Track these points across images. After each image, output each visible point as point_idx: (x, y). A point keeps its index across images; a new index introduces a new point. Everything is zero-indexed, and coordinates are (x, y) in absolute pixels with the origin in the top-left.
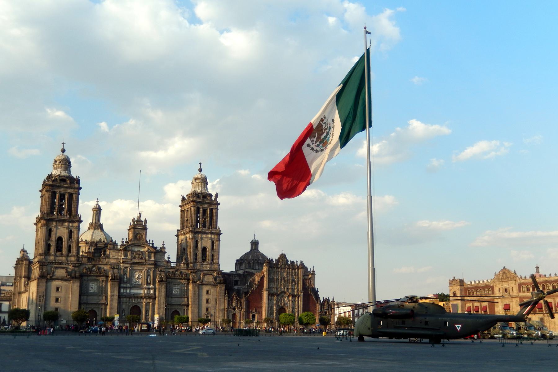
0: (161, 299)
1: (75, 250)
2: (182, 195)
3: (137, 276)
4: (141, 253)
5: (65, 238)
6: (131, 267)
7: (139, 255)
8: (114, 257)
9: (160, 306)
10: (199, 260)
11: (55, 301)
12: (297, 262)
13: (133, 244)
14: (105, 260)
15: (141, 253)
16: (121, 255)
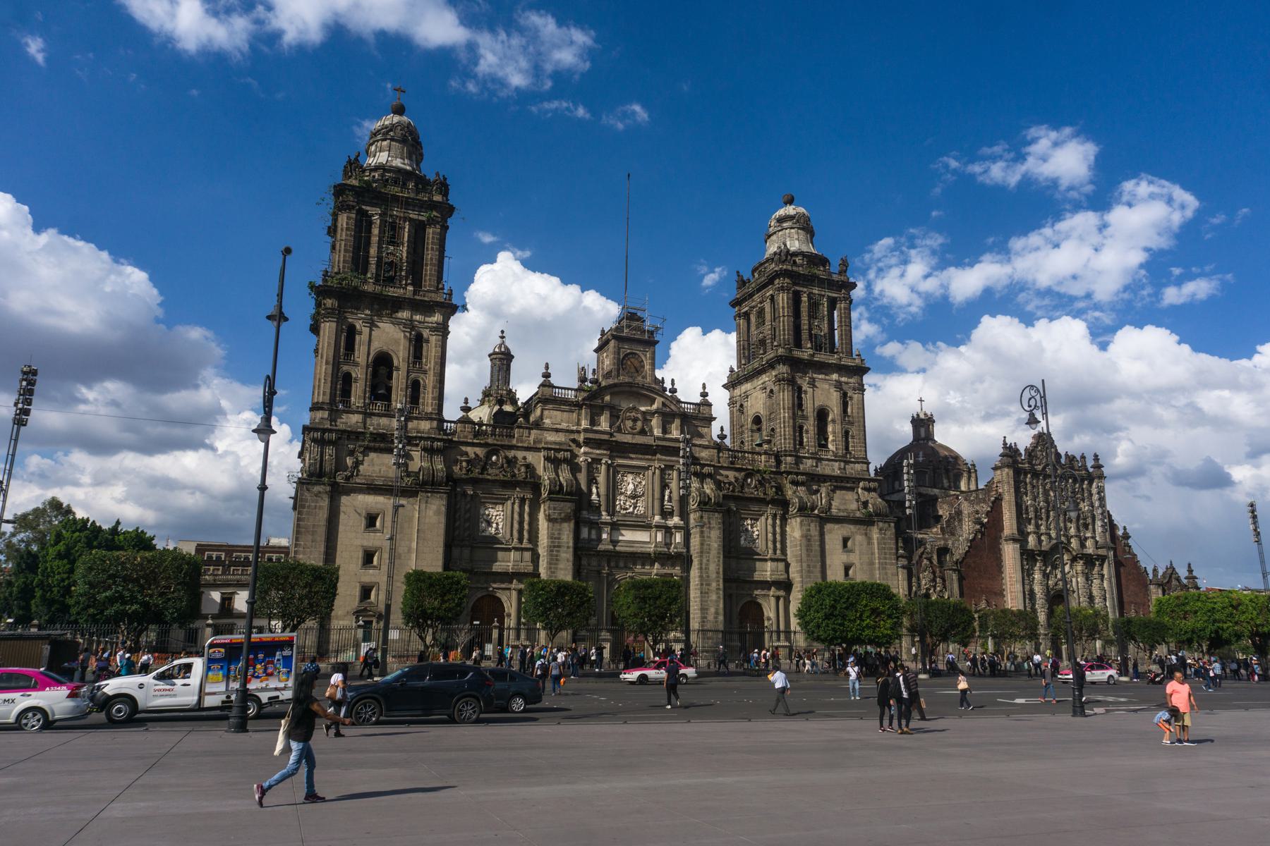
0: (708, 561)
1: (430, 395)
2: (738, 272)
3: (631, 487)
4: (639, 416)
5: (401, 356)
6: (611, 457)
7: (635, 420)
8: (558, 426)
9: (708, 585)
10: (808, 445)
11: (360, 562)
12: (1083, 457)
13: (615, 385)
14: (530, 433)
15: (639, 416)
16: (579, 420)
